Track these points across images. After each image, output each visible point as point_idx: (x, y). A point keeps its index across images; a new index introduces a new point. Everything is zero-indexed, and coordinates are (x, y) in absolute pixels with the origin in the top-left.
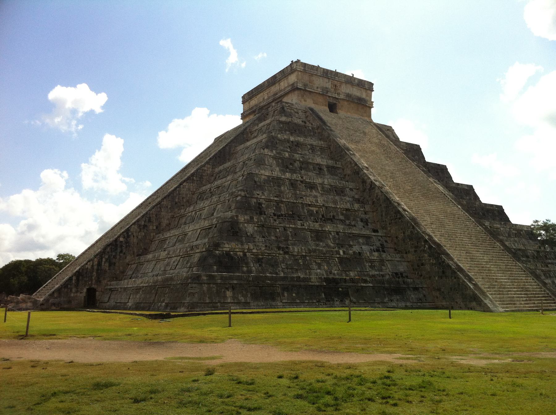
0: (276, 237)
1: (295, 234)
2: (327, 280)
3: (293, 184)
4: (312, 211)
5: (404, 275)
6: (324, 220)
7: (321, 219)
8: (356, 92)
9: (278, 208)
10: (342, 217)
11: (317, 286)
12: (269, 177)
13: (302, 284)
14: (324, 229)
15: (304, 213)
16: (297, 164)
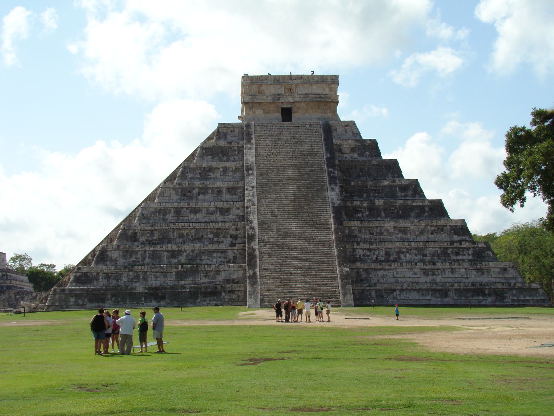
0: (136, 258)
1: (153, 255)
2: (149, 289)
3: (178, 212)
4: (183, 234)
5: (235, 281)
6: (192, 240)
7: (189, 240)
8: (317, 89)
9: (152, 234)
10: (211, 236)
11: (140, 293)
12: (156, 209)
13: (128, 291)
14: (180, 249)
15: (174, 236)
16: (195, 191)
